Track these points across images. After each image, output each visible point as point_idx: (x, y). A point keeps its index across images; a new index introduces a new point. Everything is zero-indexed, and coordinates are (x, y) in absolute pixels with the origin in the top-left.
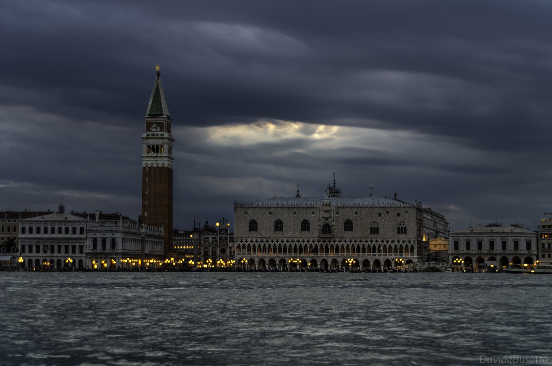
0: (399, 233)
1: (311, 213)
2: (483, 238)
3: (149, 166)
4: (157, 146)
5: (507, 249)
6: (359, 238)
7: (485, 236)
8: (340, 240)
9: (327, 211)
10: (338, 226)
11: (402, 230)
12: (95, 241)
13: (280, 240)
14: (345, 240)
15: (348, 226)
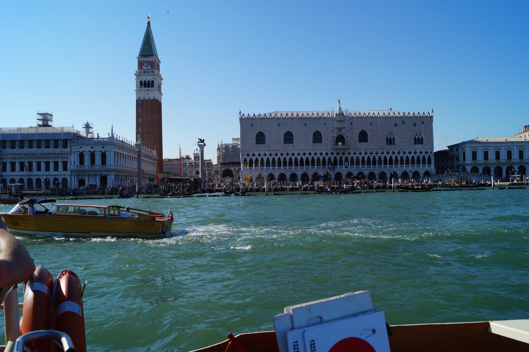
0: (415, 143)
1: (323, 124)
2: (501, 148)
3: (142, 99)
4: (149, 81)
5: (524, 158)
6: (375, 149)
7: (503, 145)
8: (355, 152)
9: (341, 121)
10: (352, 138)
11: (418, 141)
12: (81, 156)
13: (290, 154)
14: (360, 152)
15: (363, 137)
